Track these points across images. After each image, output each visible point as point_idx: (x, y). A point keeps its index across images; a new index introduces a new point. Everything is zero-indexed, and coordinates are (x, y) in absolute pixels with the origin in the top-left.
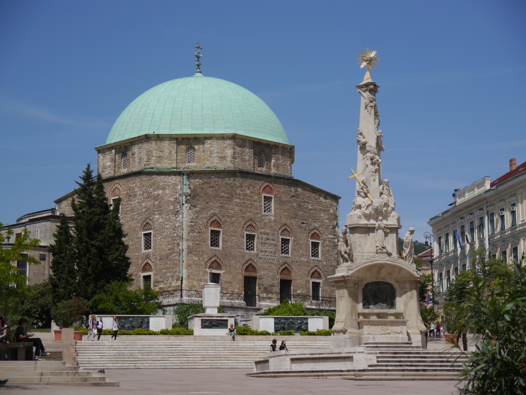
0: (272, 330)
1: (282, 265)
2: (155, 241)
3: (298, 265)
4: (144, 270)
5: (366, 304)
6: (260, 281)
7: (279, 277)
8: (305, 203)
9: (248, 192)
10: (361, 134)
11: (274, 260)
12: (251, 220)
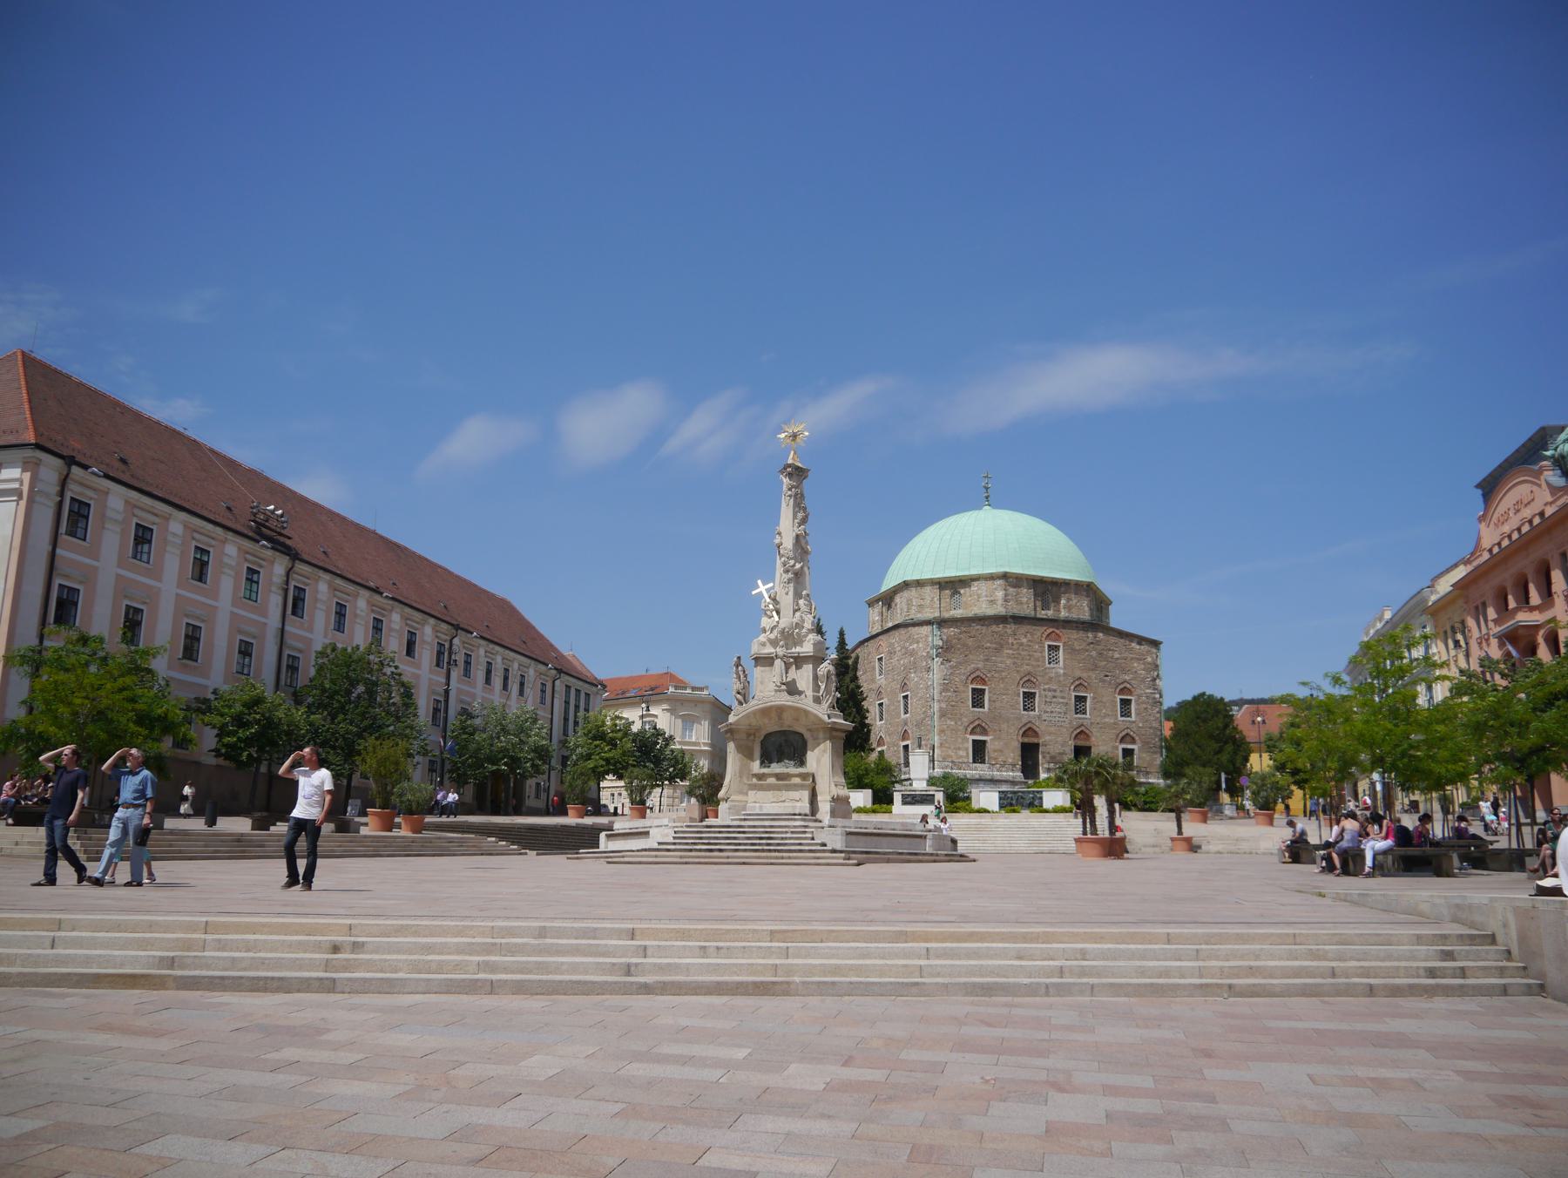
0: (996, 808)
1: (1075, 730)
2: (911, 704)
4: (904, 739)
5: (766, 759)
7: (1072, 743)
8: (1110, 650)
9: (1024, 640)
10: (779, 534)
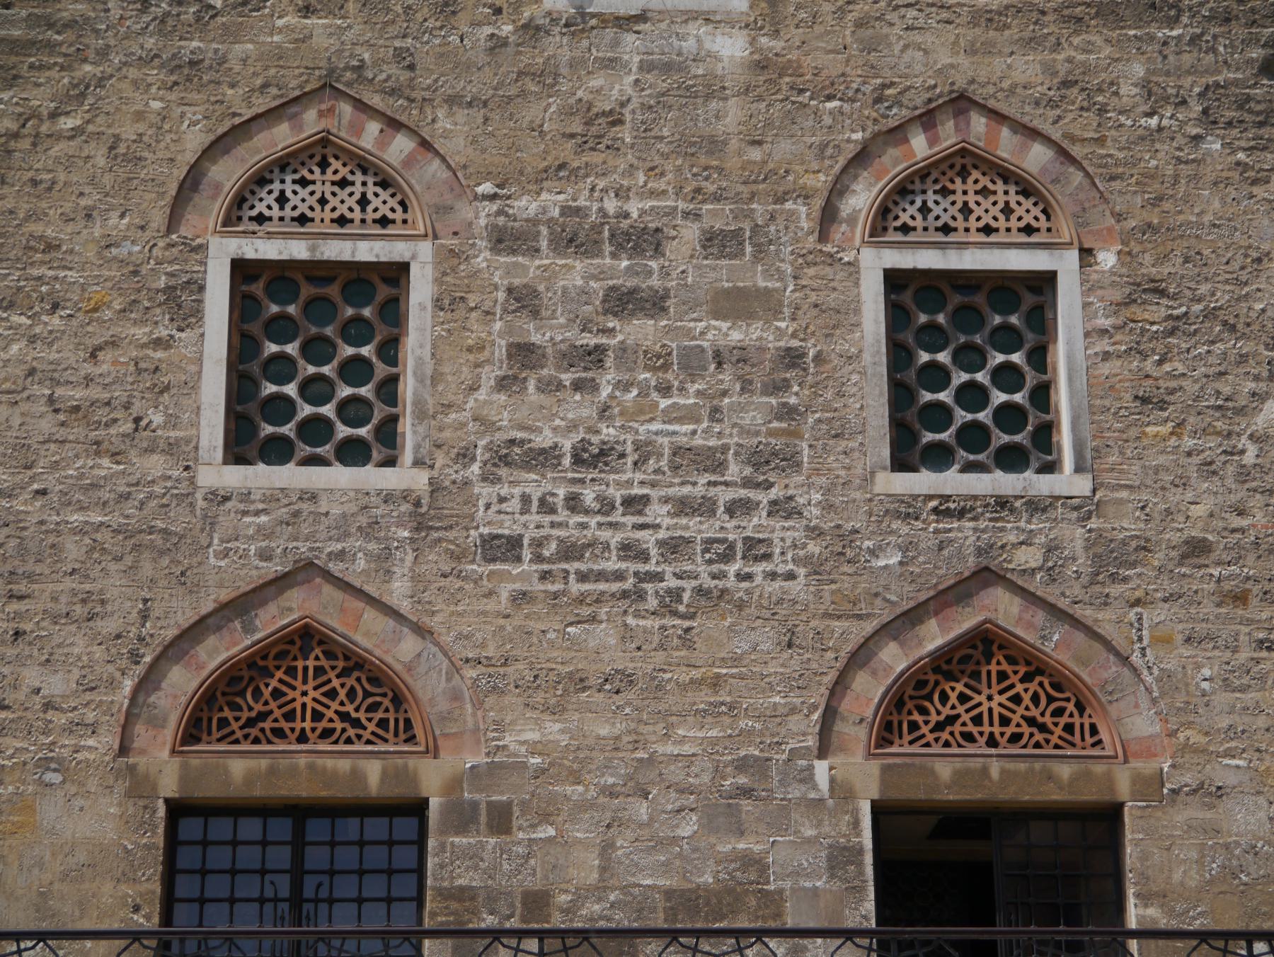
1: (912, 617)
3: (1240, 598)
6: (473, 855)
11: (756, 549)
12: (328, 88)
